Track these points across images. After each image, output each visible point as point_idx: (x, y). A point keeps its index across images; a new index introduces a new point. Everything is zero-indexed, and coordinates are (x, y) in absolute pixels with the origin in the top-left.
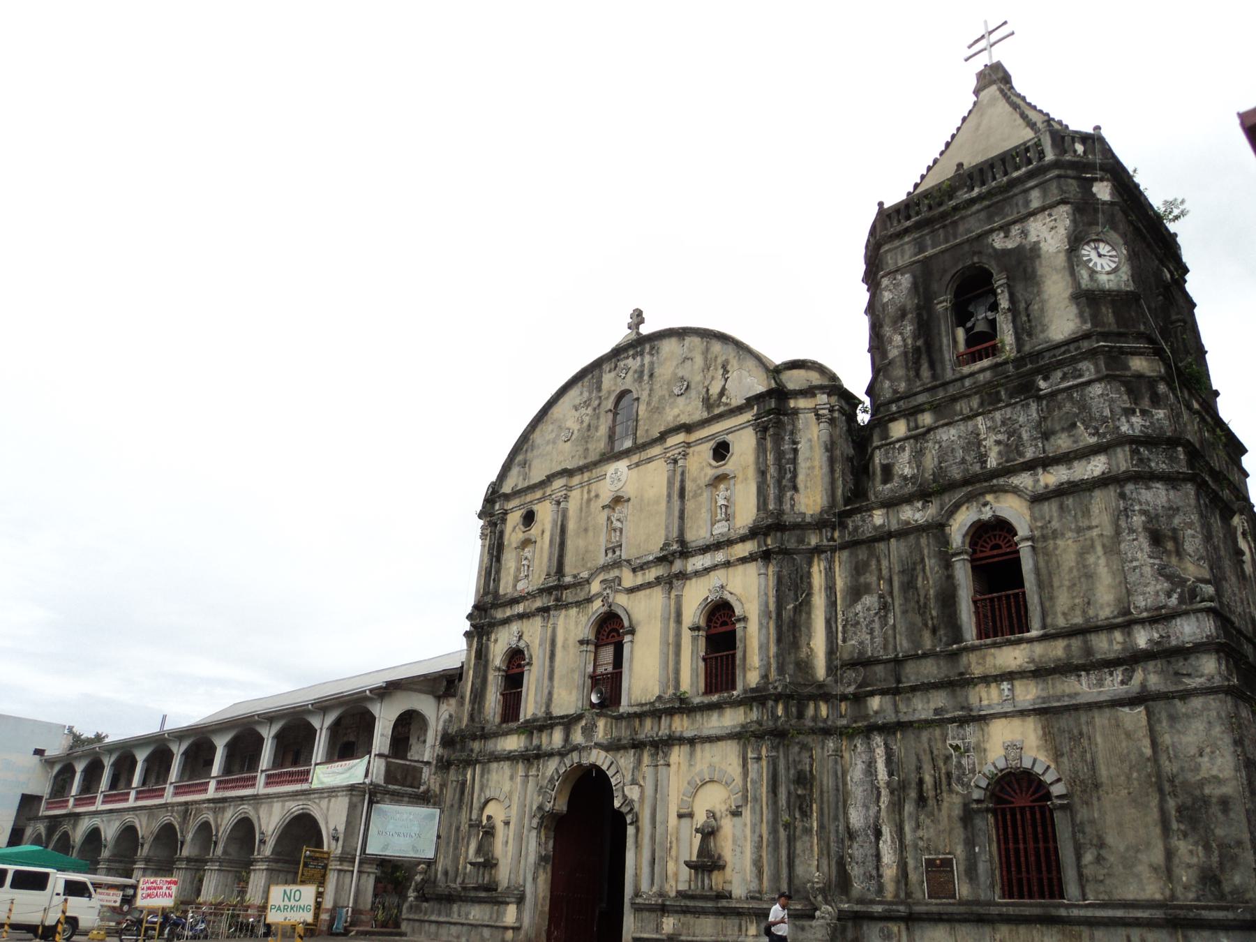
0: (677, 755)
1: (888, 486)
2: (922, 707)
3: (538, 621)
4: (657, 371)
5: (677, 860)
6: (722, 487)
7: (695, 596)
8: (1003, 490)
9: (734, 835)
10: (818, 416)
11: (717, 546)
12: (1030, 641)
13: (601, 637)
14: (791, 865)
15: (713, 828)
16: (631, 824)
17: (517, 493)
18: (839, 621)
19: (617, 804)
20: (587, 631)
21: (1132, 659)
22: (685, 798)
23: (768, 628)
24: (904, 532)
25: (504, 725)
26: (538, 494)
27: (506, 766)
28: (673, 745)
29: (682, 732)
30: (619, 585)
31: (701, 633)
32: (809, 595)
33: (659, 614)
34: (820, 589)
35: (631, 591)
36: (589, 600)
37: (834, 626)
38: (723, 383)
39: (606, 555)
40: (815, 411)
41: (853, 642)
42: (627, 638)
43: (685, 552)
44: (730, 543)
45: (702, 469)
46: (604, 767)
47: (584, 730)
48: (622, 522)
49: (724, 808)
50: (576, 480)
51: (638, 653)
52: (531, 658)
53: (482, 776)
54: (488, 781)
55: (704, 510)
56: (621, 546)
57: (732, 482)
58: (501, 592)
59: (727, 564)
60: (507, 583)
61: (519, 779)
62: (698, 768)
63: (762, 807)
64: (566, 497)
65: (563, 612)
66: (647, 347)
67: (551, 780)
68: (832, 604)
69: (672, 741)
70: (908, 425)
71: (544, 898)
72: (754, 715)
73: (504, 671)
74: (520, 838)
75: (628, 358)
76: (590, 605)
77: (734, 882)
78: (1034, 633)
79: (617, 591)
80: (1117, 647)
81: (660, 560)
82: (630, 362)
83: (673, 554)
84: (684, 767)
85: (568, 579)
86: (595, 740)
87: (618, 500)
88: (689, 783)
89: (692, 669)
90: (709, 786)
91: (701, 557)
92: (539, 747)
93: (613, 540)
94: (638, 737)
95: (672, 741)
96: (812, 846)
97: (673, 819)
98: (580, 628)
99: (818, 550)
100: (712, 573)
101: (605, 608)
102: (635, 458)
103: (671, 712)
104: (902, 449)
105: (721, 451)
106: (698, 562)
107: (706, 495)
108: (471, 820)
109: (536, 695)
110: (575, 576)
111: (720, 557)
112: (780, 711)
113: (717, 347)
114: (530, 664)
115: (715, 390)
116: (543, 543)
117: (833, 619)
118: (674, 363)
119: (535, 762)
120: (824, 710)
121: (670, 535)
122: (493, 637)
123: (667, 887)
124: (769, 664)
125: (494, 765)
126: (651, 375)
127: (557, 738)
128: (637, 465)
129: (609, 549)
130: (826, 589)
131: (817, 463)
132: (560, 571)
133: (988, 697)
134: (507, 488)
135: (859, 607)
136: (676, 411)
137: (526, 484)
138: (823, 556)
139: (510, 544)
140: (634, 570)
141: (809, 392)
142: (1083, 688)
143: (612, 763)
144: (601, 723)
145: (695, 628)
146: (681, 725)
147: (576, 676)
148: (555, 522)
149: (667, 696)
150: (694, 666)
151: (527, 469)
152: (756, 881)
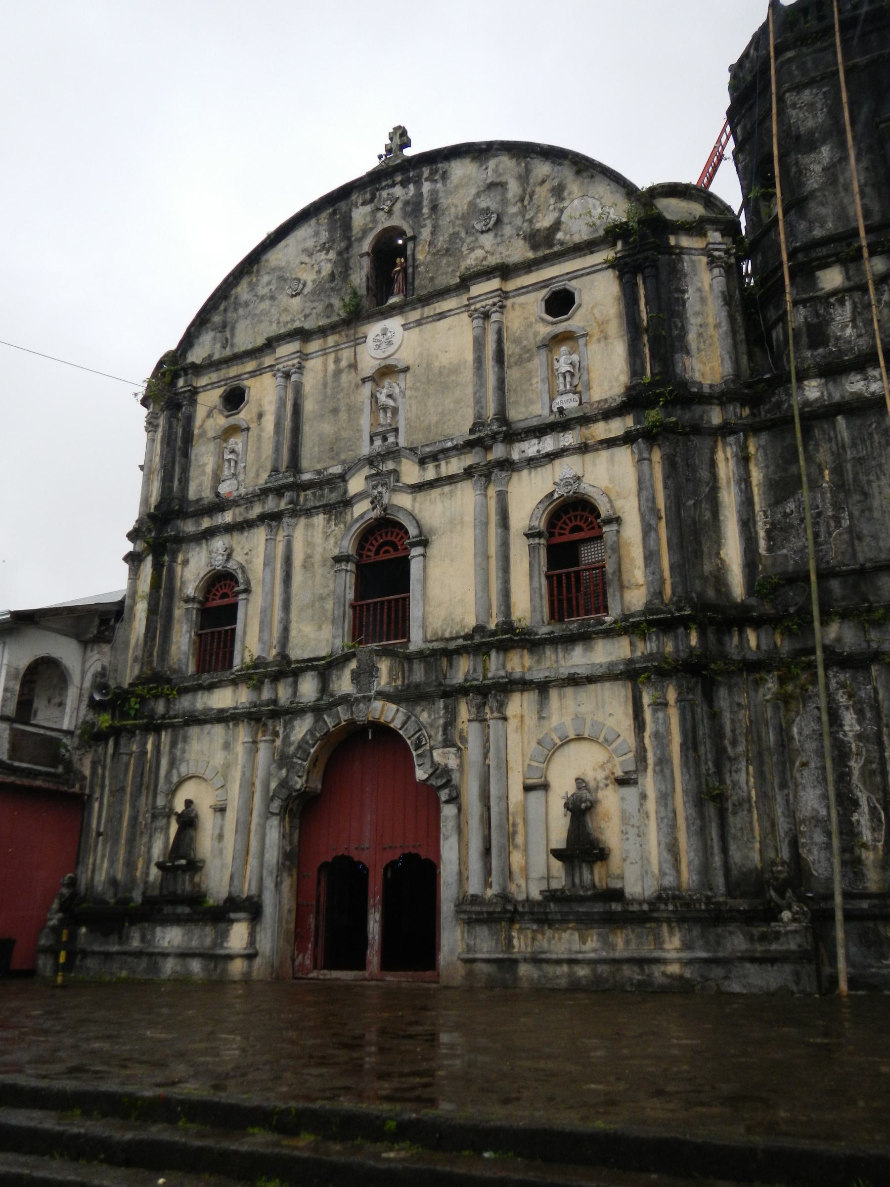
1: (821, 351)
3: (260, 535)
4: (444, 202)
5: (526, 850)
6: (564, 349)
9: (623, 811)
10: (713, 262)
11: (562, 425)
13: (364, 552)
14: (725, 850)
15: (591, 802)
16: (447, 802)
17: (211, 365)
18: (760, 524)
19: (421, 774)
20: (345, 543)
22: (535, 764)
23: (656, 531)
25: (205, 676)
26: (251, 366)
27: (218, 731)
28: (512, 691)
29: (524, 673)
30: (398, 481)
31: (542, 541)
32: (715, 489)
33: (469, 518)
34: (728, 482)
36: (347, 503)
37: (752, 530)
38: (556, 215)
39: (372, 442)
40: (707, 252)
41: (785, 551)
42: (416, 551)
43: (512, 435)
44: (585, 420)
46: (396, 724)
47: (356, 677)
48: (394, 400)
49: (601, 775)
50: (314, 346)
51: (436, 569)
52: (248, 582)
53: (173, 744)
54: (184, 751)
55: (534, 381)
56: (396, 430)
57: (582, 341)
58: (192, 495)
59: (583, 449)
60: (201, 484)
61: (240, 749)
62: (555, 720)
63: (672, 772)
64: (300, 368)
65: (303, 521)
66: (426, 172)
67: (303, 745)
68: (747, 502)
70: (847, 273)
71: (289, 911)
72: (645, 648)
73: (200, 602)
74: (244, 828)
75: (393, 185)
76: (349, 512)
77: (627, 875)
79: (394, 490)
81: (469, 445)
82: (398, 191)
83: (494, 437)
84: (531, 720)
85: (306, 477)
86: (375, 688)
87: (387, 371)
88: (539, 743)
89: (532, 590)
90: (573, 747)
91: (536, 441)
92: (275, 701)
93: (382, 421)
94: (448, 682)
96: (751, 823)
97: (516, 793)
98: (332, 541)
99: (725, 430)
100: (557, 462)
101: (377, 513)
102: (415, 315)
103: (504, 647)
104: (842, 303)
106: (531, 448)
107: (539, 362)
108: (154, 807)
109: (261, 631)
110: (319, 472)
111: (569, 439)
112: (694, 641)
113: (542, 169)
114: (247, 591)
115: (544, 222)
116: (262, 430)
117: (751, 521)
118: (473, 191)
119: (270, 722)
120: (752, 638)
121: (483, 412)
122: (180, 558)
123: (513, 888)
124: (662, 581)
126: (434, 208)
127: (308, 688)
128: (419, 323)
129: (376, 434)
130: (739, 483)
131: (711, 321)
132: (295, 465)
134: (196, 356)
135: (791, 506)
136: (479, 253)
137: (228, 352)
138: (731, 439)
139: (203, 434)
140: (422, 462)
141: (696, 228)
143: (409, 718)
144: (384, 666)
145: (530, 535)
147: (329, 605)
148: (282, 403)
149: (492, 626)
150: (536, 584)
152: (673, 872)
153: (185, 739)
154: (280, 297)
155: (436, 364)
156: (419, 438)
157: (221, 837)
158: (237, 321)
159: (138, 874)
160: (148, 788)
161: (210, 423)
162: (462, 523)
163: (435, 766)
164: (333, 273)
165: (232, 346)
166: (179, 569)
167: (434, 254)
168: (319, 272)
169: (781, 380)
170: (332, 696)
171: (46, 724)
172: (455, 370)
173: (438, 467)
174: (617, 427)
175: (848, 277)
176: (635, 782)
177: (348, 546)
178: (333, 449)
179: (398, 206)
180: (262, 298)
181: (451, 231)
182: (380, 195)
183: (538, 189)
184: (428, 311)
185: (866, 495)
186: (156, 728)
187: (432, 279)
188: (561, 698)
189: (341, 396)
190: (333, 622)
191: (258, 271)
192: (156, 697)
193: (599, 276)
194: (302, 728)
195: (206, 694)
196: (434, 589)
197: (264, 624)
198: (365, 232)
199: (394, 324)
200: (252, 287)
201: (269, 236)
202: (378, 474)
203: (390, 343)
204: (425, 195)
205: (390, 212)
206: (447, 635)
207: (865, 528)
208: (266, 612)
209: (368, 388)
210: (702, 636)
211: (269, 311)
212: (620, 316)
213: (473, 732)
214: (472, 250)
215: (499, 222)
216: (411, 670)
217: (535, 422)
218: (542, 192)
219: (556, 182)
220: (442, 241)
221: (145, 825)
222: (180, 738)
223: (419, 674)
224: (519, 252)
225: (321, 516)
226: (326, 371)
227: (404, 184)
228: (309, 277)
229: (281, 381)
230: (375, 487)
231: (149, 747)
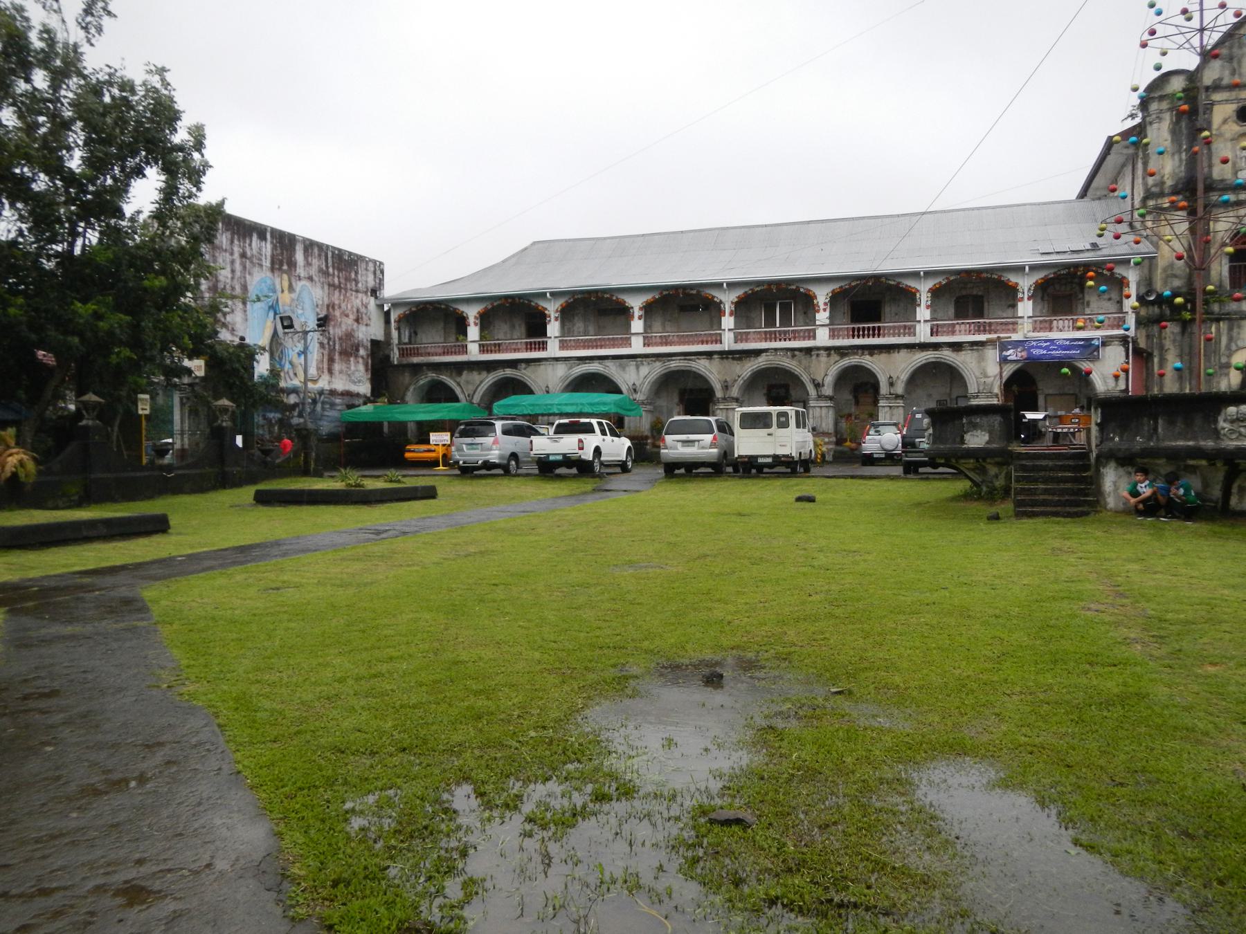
53: (1230, 329)
54: (1239, 333)
137: (1237, 80)
139: (1220, 135)
151: (1235, 64)
153: (1239, 327)
160: (1215, 352)
161: (1226, 127)
165: (1240, 75)
186: (1218, 320)
192: (1214, 301)
231: (1213, 329)
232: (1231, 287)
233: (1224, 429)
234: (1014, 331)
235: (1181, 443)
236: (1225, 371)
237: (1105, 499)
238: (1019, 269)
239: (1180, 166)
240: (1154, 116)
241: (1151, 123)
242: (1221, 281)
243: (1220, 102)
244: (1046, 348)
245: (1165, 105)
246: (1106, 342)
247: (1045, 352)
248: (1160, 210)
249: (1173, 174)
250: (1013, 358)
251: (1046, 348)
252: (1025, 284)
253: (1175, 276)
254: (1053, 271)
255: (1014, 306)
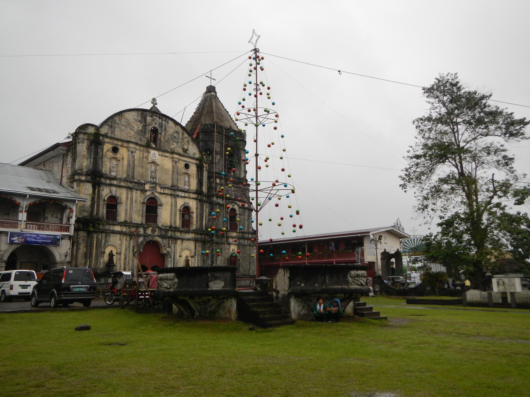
0: (179, 242)
2: (219, 240)
4: (167, 129)
7: (180, 202)
8: (236, 204)
10: (206, 170)
12: (237, 232)
21: (249, 239)
24: (219, 204)
26: (120, 143)
27: (118, 236)
33: (170, 203)
35: (161, 193)
36: (146, 191)
44: (190, 193)
45: (182, 168)
50: (138, 147)
53: (106, 237)
54: (109, 239)
56: (156, 178)
59: (190, 198)
62: (184, 246)
66: (164, 119)
69: (179, 239)
75: (157, 116)
78: (238, 231)
80: (247, 237)
84: (180, 245)
85: (136, 180)
87: (154, 162)
95: (179, 239)
98: (142, 198)
99: (206, 202)
102: (161, 153)
103: (178, 231)
105: (187, 166)
106: (181, 194)
110: (138, 180)
111: (187, 195)
115: (186, 147)
118: (173, 131)
125: (112, 235)
128: (162, 156)
133: (231, 240)
135: (211, 217)
137: (113, 135)
139: (106, 155)
140: (161, 188)
142: (242, 241)
146: (178, 234)
147: (141, 212)
153: (109, 236)
154: (128, 128)
155: (164, 167)
156: (160, 182)
157: (120, 259)
158: (115, 127)
159: (98, 266)
160: (100, 246)
161: (108, 153)
162: (168, 204)
163: (167, 251)
164: (142, 130)
165: (114, 134)
166: (101, 191)
167: (165, 141)
168: (138, 127)
169: (213, 196)
170: (147, 234)
171: (52, 222)
172: (168, 170)
173: (164, 190)
174: (194, 196)
175: (220, 182)
176: (194, 257)
177: (146, 200)
178: (142, 176)
179: (158, 123)
180: (123, 125)
181: (168, 137)
182: (154, 117)
183: (185, 139)
184: (163, 154)
185: (219, 218)
186: (102, 232)
187: (164, 146)
188: (185, 242)
189: (144, 164)
190: (142, 216)
191: (121, 116)
192: (101, 224)
193: (193, 165)
194: (141, 239)
195: (113, 227)
196: (163, 216)
197: (126, 213)
198: (150, 125)
199: (156, 153)
200: (120, 120)
201: (127, 110)
202: (153, 187)
203: (156, 157)
204: (164, 124)
205: (156, 123)
206: (164, 225)
207: (218, 223)
208: (126, 210)
209: (150, 165)
210: (204, 237)
211: (124, 130)
212: (196, 175)
213: (173, 246)
214: (172, 144)
215: (178, 142)
216: (162, 232)
217: (182, 189)
218: (186, 140)
219: (188, 140)
220: (166, 138)
221: (100, 255)
222: (108, 236)
223: (163, 233)
224: (181, 151)
225: (139, 191)
226: (140, 155)
227: (159, 118)
228: (136, 127)
229: (130, 153)
230: (153, 190)
232: (107, 219)
233: (350, 280)
234: (16, 227)
235: (336, 287)
236: (103, 255)
237: (291, 314)
238: (23, 196)
239: (90, 164)
240: (81, 140)
241: (79, 143)
242: (103, 216)
243: (107, 142)
244: (35, 238)
245: (85, 137)
246: (63, 237)
247: (34, 240)
248: (81, 181)
249: (87, 167)
250: (17, 241)
251: (34, 238)
252: (24, 204)
253: (85, 211)
254: (38, 200)
255: (17, 215)
